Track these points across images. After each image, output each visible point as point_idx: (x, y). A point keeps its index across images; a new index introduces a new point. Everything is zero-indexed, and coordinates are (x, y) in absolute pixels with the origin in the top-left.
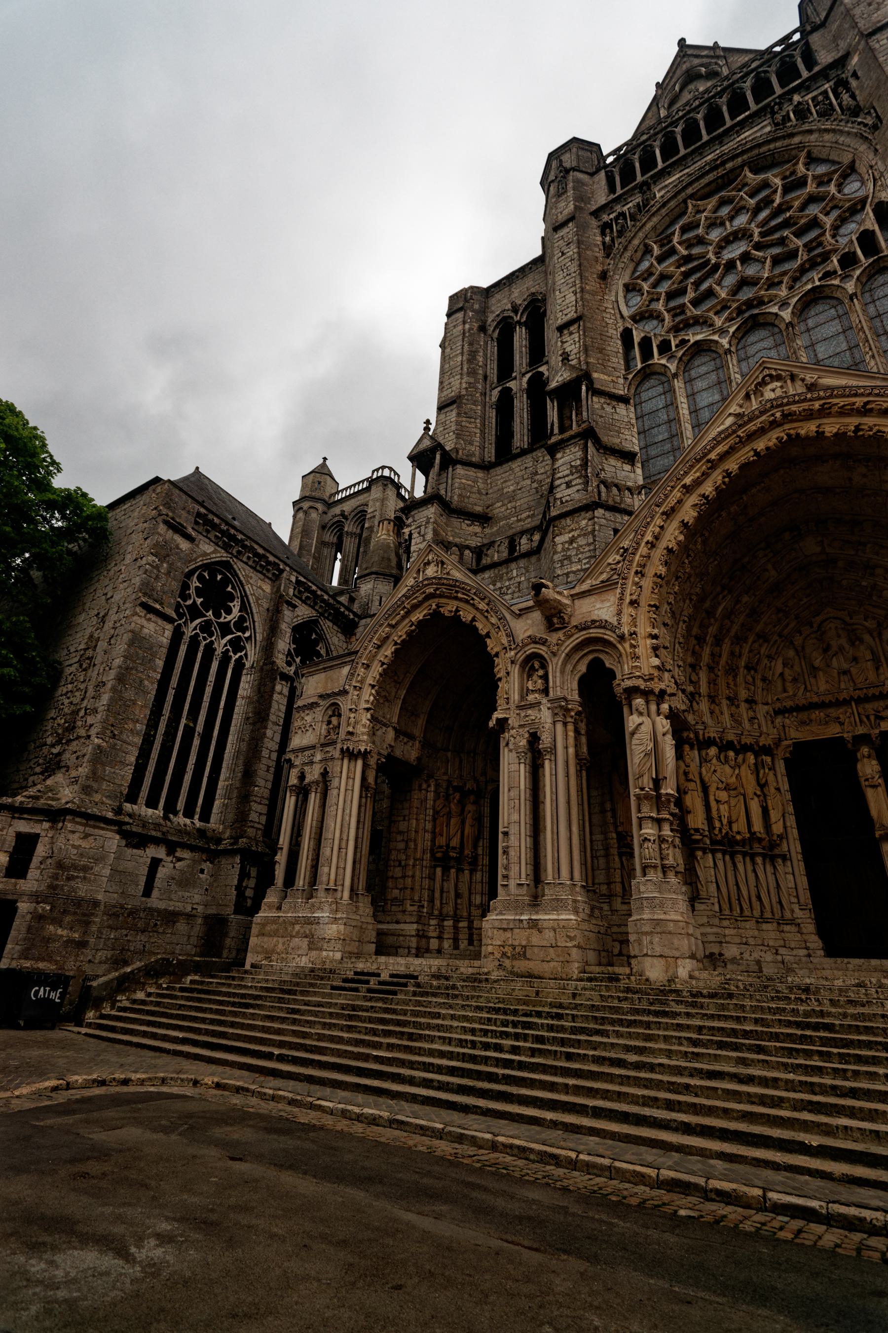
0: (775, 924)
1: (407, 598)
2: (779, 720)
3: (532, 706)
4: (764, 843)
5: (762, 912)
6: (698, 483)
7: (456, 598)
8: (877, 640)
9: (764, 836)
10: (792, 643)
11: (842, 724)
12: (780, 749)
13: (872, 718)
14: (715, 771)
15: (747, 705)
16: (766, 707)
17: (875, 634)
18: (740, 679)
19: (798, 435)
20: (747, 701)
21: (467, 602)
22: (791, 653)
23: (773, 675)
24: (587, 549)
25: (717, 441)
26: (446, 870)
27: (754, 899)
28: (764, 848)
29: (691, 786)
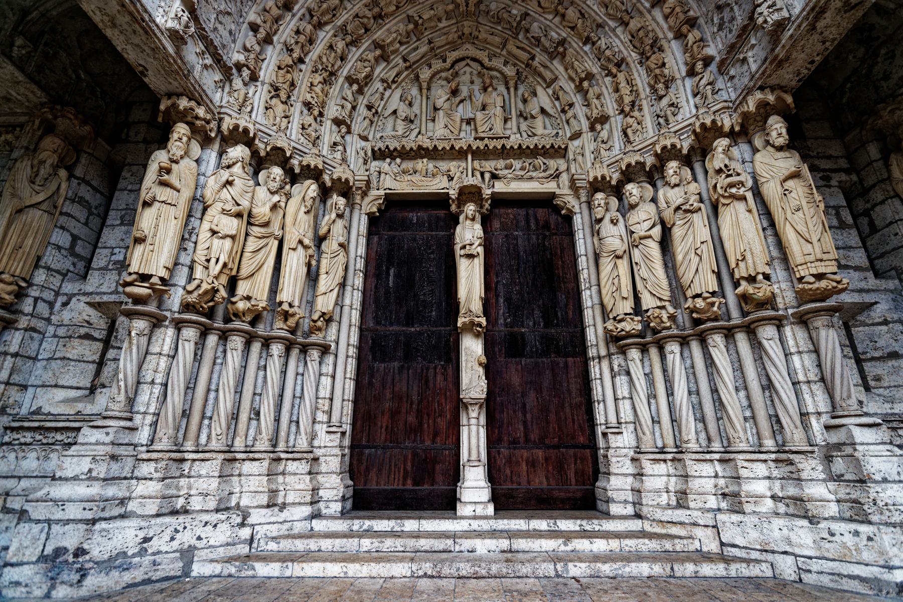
0: (266, 463)
2: (374, 165)
4: (292, 322)
5: (255, 439)
8: (512, 90)
9: (300, 312)
10: (417, 77)
11: (451, 179)
12: (367, 200)
13: (487, 176)
14: (229, 183)
15: (334, 127)
16: (363, 143)
17: (512, 83)
18: (335, 90)
20: (338, 122)
22: (415, 91)
23: (384, 108)
27: (244, 417)
28: (293, 331)
29: (164, 194)
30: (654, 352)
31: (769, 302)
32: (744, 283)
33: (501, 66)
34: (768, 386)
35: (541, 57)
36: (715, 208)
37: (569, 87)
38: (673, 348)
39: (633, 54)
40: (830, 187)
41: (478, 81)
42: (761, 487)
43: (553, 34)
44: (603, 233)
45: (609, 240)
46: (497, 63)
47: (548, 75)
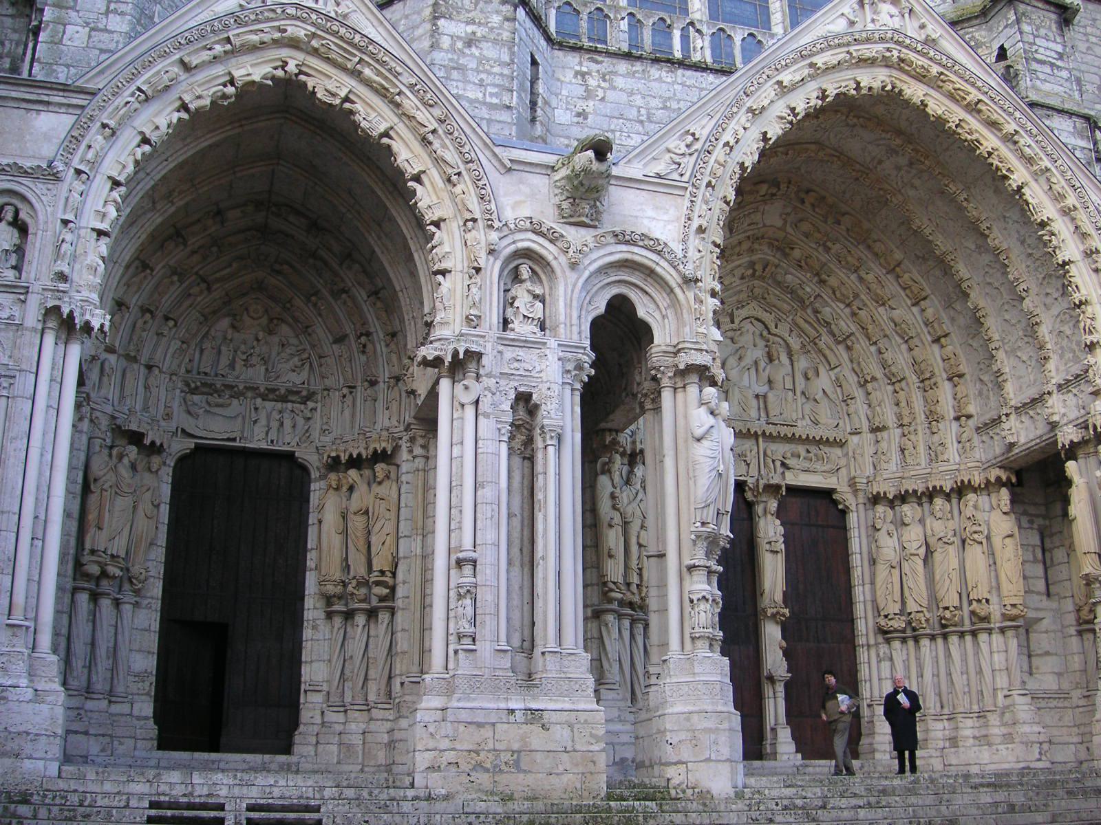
1: (239, 22)
3: (526, 344)
6: (794, 87)
7: (356, 74)
19: (901, 91)
21: (382, 92)
24: (496, 70)
25: (829, 43)
26: (95, 597)
30: (911, 643)
31: (986, 619)
32: (974, 602)
33: (786, 335)
34: (980, 672)
35: (826, 338)
36: (964, 541)
37: (853, 379)
38: (925, 642)
39: (914, 377)
40: (1032, 528)
41: (761, 343)
42: (968, 732)
43: (842, 323)
44: (881, 543)
45: (885, 551)
46: (783, 330)
47: (834, 362)
